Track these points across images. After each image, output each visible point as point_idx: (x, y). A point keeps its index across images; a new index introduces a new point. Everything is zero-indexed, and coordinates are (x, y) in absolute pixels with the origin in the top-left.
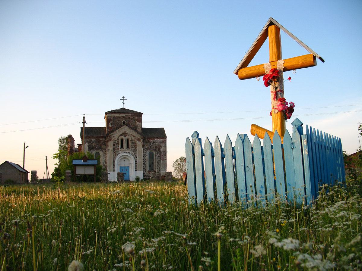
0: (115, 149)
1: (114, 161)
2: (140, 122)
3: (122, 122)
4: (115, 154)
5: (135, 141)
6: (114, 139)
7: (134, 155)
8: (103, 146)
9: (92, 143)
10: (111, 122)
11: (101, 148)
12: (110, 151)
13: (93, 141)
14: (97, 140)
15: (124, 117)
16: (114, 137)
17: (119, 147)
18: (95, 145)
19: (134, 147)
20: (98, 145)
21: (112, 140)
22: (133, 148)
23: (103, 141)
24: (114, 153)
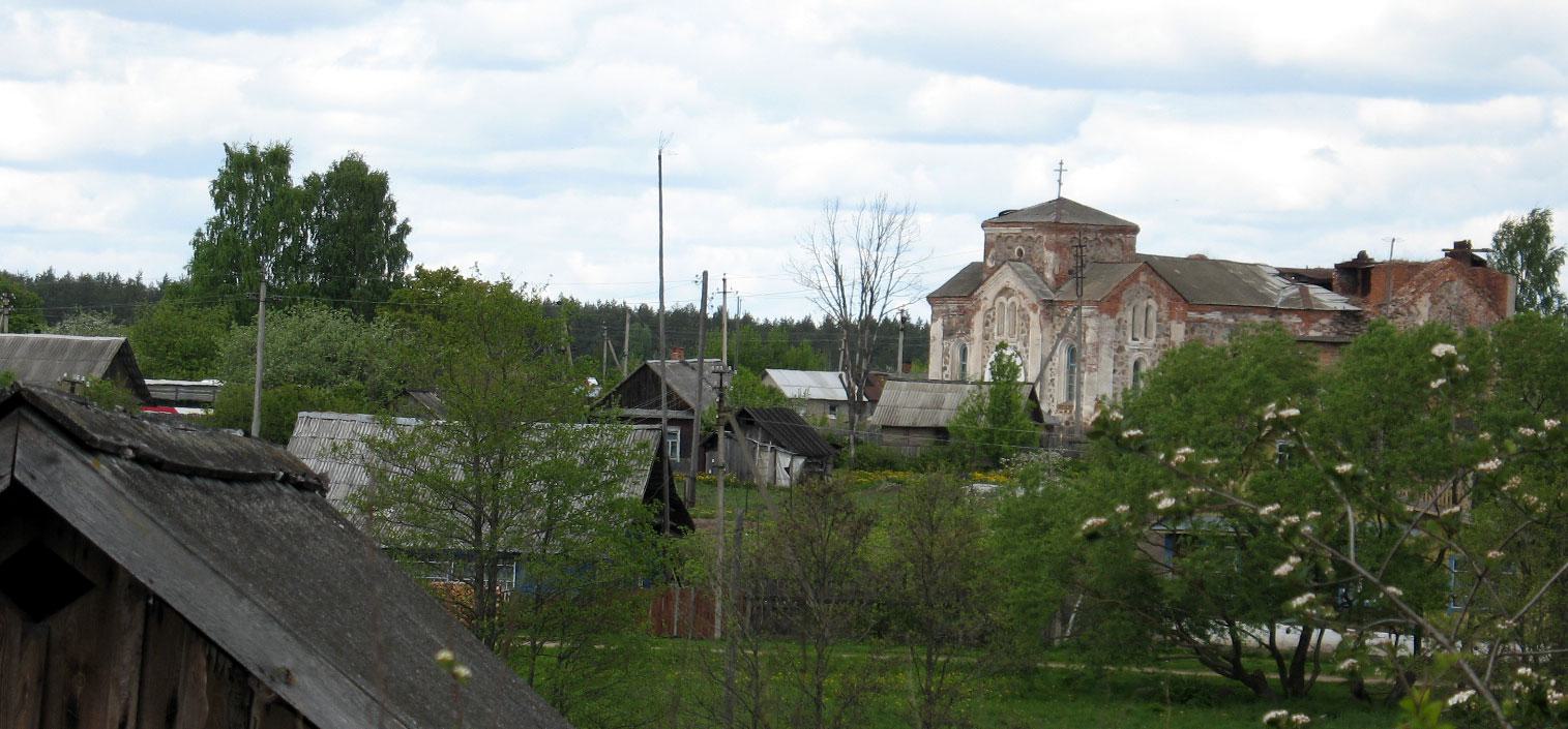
16: (986, 299)
20: (963, 322)
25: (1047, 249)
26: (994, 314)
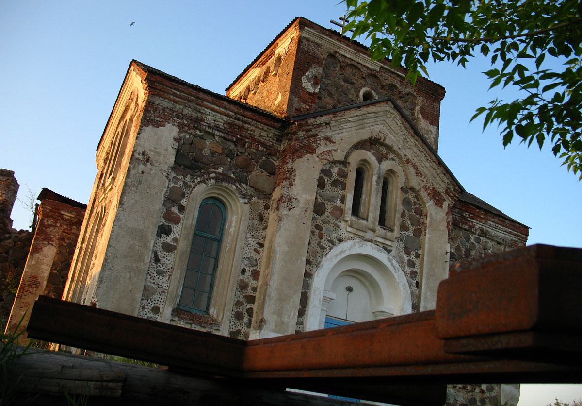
0: (323, 204)
1: (308, 275)
2: (431, 123)
3: (361, 94)
4: (321, 236)
5: (417, 197)
6: (329, 152)
7: (408, 270)
8: (257, 175)
9: (201, 138)
10: (316, 70)
11: (241, 180)
12: (296, 212)
13: (209, 126)
14: (231, 125)
15: (373, 75)
16: (328, 139)
17: (343, 200)
18: (213, 153)
19: (411, 228)
20: (230, 155)
21: (318, 151)
22: (407, 229)
23: (263, 144)
24: (317, 227)
25: (424, 118)
26: (344, 175)
